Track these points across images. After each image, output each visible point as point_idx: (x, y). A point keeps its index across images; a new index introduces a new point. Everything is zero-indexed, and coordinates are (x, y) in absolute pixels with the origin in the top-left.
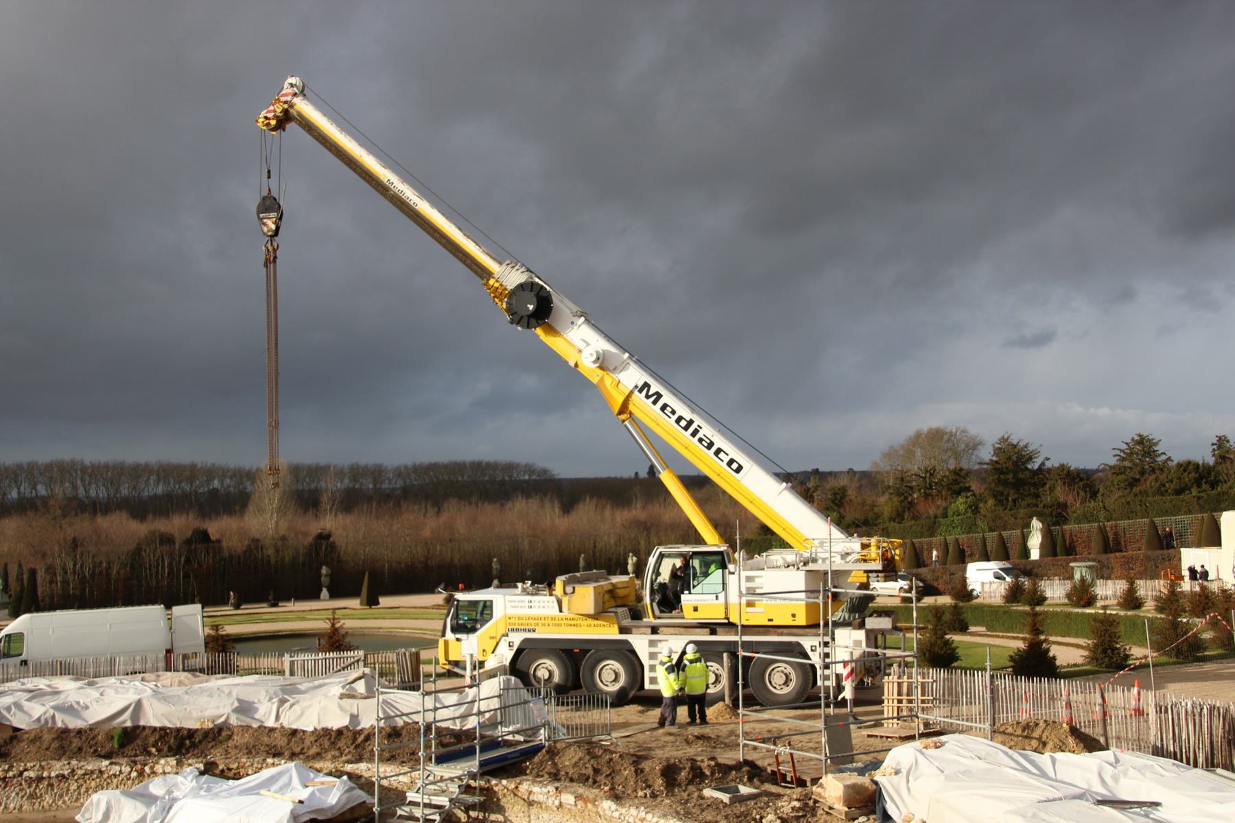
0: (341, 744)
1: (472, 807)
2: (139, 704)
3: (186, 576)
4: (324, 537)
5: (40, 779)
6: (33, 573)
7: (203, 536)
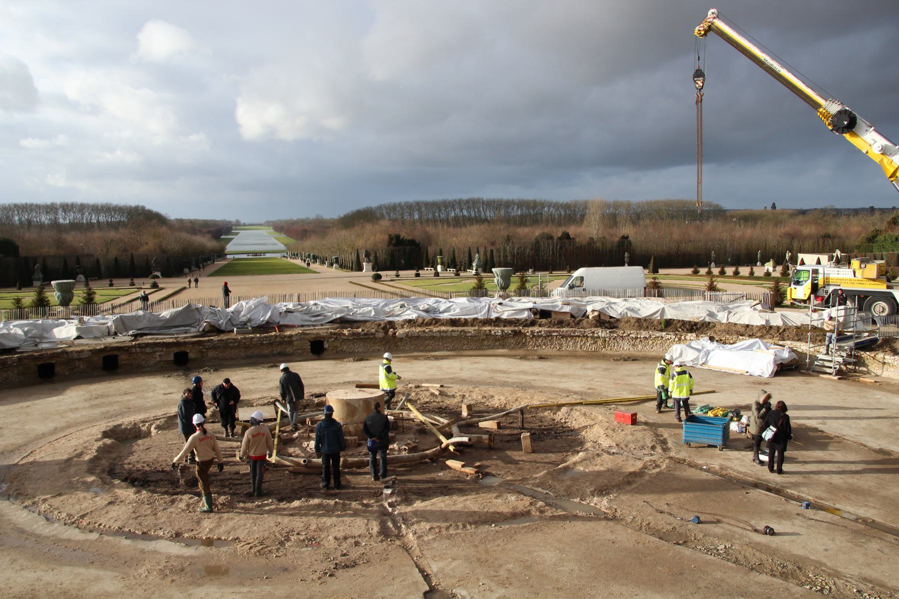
0: (772, 332)
1: (850, 364)
2: (663, 309)
3: (560, 255)
4: (625, 238)
5: (637, 338)
6: (492, 251)
7: (566, 236)
